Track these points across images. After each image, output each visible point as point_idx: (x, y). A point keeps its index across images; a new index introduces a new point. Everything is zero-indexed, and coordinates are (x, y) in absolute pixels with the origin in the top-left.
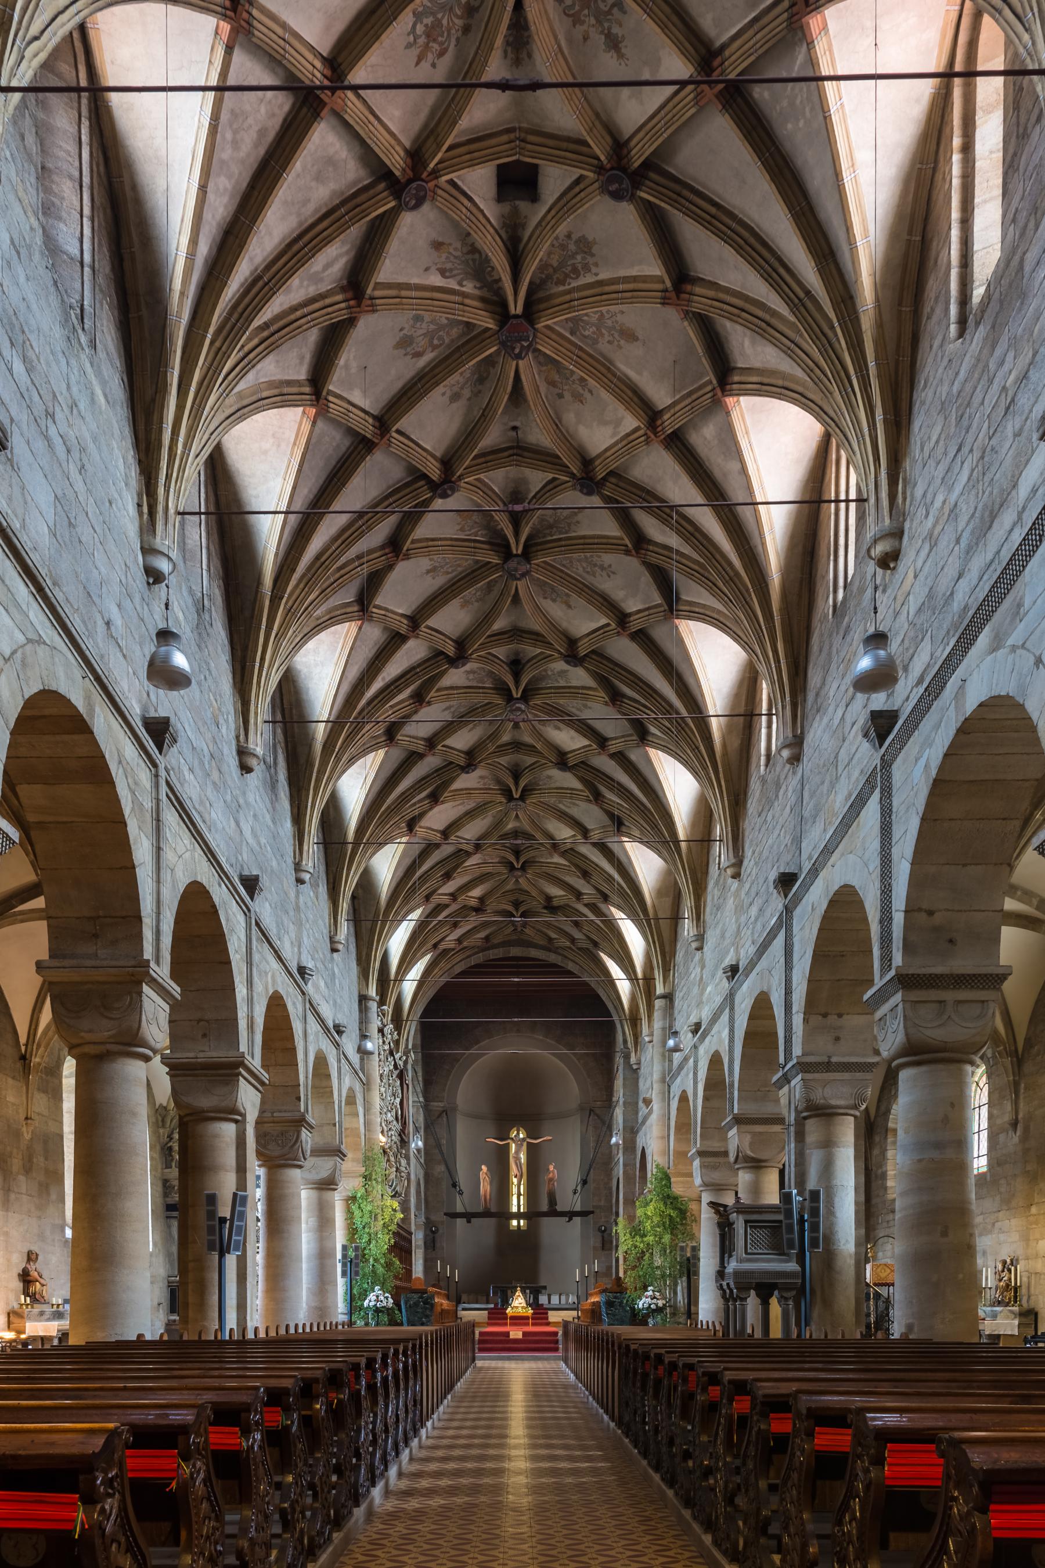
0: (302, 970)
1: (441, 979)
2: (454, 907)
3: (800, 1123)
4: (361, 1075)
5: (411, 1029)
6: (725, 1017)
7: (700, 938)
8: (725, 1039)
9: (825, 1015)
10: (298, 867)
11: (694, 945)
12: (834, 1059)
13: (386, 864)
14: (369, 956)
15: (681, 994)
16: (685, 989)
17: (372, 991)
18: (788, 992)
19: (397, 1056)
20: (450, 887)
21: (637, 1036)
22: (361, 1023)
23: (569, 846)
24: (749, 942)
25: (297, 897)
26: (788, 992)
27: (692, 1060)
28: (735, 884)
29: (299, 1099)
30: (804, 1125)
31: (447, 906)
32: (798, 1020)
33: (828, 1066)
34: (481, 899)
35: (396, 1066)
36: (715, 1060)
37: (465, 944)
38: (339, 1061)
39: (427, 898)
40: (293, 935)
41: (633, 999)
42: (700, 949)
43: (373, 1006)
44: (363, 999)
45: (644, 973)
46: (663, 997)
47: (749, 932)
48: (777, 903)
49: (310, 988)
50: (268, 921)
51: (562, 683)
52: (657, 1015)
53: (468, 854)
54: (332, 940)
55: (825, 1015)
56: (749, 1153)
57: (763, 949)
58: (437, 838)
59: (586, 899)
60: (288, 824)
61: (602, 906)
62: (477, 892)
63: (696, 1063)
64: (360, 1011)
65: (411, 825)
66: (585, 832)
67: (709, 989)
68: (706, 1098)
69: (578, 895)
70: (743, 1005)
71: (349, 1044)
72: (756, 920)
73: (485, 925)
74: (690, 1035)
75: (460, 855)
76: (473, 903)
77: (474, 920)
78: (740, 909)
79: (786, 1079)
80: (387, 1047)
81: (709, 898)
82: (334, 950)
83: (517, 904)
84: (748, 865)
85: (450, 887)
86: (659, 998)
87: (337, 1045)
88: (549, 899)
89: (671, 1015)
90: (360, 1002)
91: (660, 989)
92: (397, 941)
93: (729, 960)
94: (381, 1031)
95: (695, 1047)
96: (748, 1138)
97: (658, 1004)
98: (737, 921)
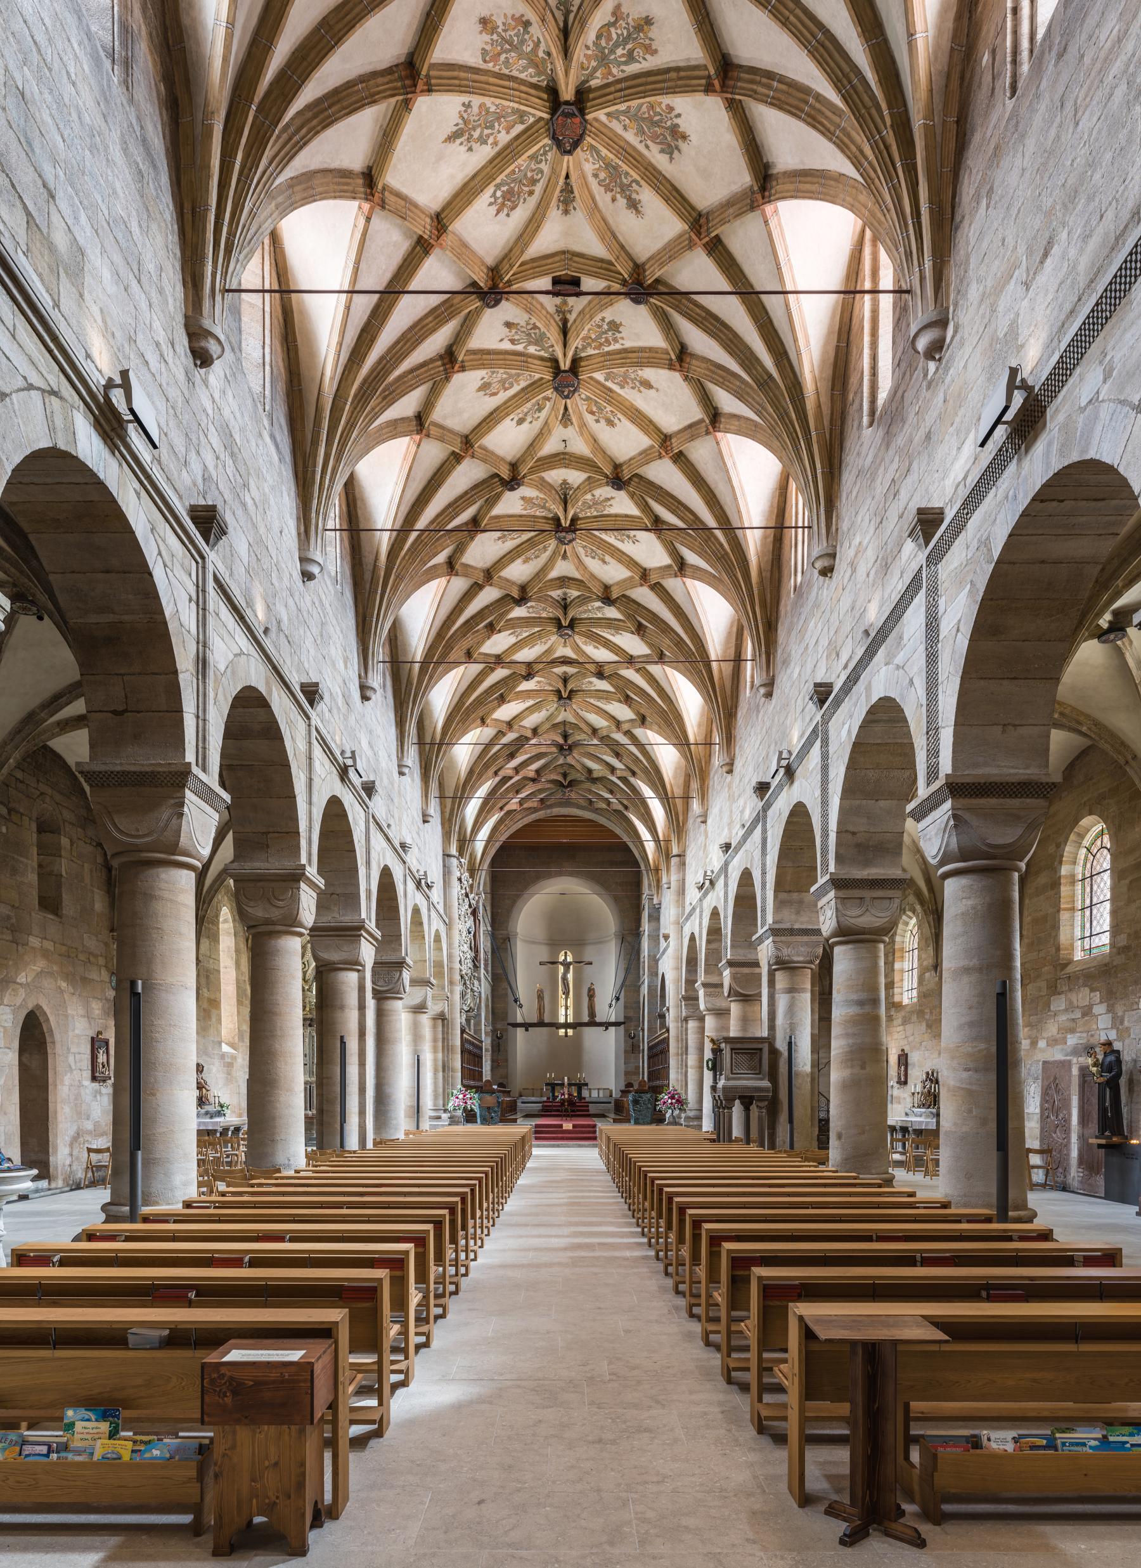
0: (403, 846)
5: (483, 876)
8: (723, 898)
11: (700, 820)
13: (463, 753)
17: (454, 851)
18: (764, 873)
19: (471, 896)
22: (444, 875)
26: (764, 873)
27: (698, 910)
31: (511, 778)
34: (538, 771)
35: (470, 906)
36: (715, 913)
37: (525, 806)
38: (429, 910)
39: (496, 773)
42: (704, 822)
44: (447, 856)
49: (407, 859)
50: (381, 815)
51: (600, 615)
52: (673, 869)
59: (619, 773)
61: (632, 780)
62: (535, 766)
63: (701, 912)
68: (708, 942)
69: (613, 769)
71: (436, 895)
73: (540, 791)
76: (532, 775)
82: (425, 821)
83: (565, 775)
87: (428, 898)
88: (590, 771)
89: (684, 870)
91: (675, 851)
92: (472, 809)
94: (460, 879)
95: (701, 900)
97: (674, 861)
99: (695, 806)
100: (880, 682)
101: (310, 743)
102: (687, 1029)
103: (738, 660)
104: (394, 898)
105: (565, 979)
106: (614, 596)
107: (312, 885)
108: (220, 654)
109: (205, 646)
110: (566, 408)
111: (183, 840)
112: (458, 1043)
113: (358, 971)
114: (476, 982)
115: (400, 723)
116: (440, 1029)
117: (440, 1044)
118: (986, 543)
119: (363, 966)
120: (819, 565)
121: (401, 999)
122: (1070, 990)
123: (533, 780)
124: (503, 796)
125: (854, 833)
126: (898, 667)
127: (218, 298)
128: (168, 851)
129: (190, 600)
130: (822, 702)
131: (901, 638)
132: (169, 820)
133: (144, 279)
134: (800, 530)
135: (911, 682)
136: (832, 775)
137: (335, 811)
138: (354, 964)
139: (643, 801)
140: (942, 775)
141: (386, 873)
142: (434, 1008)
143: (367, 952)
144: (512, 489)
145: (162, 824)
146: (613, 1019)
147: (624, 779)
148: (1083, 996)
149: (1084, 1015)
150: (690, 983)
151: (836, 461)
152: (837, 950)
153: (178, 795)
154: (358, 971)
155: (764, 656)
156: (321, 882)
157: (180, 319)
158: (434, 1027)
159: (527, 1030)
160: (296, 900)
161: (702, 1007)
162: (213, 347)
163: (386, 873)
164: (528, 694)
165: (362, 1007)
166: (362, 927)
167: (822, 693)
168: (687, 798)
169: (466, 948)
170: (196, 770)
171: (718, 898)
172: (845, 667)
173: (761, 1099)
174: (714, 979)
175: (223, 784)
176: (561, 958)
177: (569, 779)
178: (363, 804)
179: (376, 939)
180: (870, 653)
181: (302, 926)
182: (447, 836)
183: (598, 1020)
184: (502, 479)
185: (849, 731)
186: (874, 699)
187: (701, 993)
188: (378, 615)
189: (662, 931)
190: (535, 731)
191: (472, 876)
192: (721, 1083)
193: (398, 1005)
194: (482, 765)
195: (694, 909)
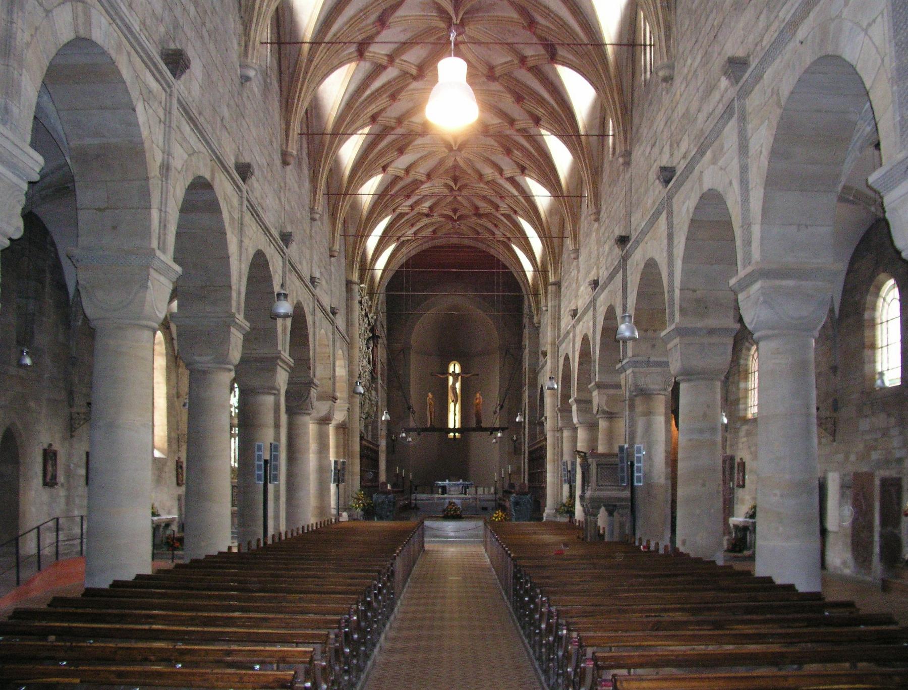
0: (313, 280)
1: (402, 258)
4: (347, 337)
5: (381, 297)
6: (591, 312)
7: (577, 251)
10: (312, 210)
11: (572, 256)
12: (652, 359)
14: (353, 252)
17: (355, 277)
19: (370, 316)
20: (410, 202)
21: (538, 303)
22: (347, 300)
23: (490, 178)
24: (604, 268)
25: (311, 230)
27: (571, 335)
28: (596, 225)
29: (309, 368)
31: (407, 214)
33: (648, 363)
34: (431, 208)
35: (369, 324)
36: (585, 339)
39: (394, 210)
40: (308, 257)
41: (534, 278)
42: (577, 258)
43: (356, 288)
44: (349, 284)
48: (617, 251)
49: (317, 292)
50: (295, 258)
53: (422, 183)
54: (331, 250)
57: (611, 277)
58: (402, 173)
60: (307, 185)
61: (514, 216)
63: (574, 337)
64: (347, 292)
65: (384, 168)
66: (501, 171)
67: (582, 288)
68: (580, 364)
70: (601, 309)
71: (340, 321)
72: (609, 254)
73: (433, 224)
75: (417, 183)
76: (426, 211)
77: (425, 221)
78: (598, 241)
80: (363, 313)
82: (331, 256)
83: (455, 211)
84: (603, 215)
85: (410, 202)
88: (477, 208)
89: (560, 297)
90: (347, 285)
91: (552, 279)
92: (372, 243)
93: (592, 276)
94: (360, 302)
95: (574, 326)
96: (605, 398)
99: (569, 243)
102: (562, 438)
103: (603, 135)
105: (454, 388)
106: (497, 74)
107: (240, 328)
108: (179, 157)
111: (147, 308)
112: (357, 448)
113: (275, 394)
114: (374, 393)
115: (314, 179)
118: (776, 92)
119: (279, 390)
121: (309, 414)
122: (873, 414)
124: (399, 229)
125: (694, 291)
129: (160, 121)
130: (667, 182)
131: (722, 148)
134: (648, 48)
135: (731, 183)
136: (676, 242)
137: (259, 263)
138: (272, 390)
140: (753, 261)
143: (282, 378)
148: (880, 420)
149: (884, 435)
150: (566, 396)
152: (683, 386)
154: (275, 394)
155: (622, 134)
156: (247, 325)
159: (419, 434)
161: (575, 420)
165: (277, 426)
166: (279, 358)
167: (667, 175)
168: (562, 238)
169: (365, 362)
170: (158, 253)
171: (588, 328)
172: (684, 157)
173: (622, 507)
175: (175, 260)
176: (451, 369)
177: (458, 214)
178: (282, 254)
180: (701, 152)
182: (350, 266)
183: (484, 425)
185: (688, 210)
186: (705, 189)
187: (574, 408)
188: (299, 97)
191: (371, 299)
192: (588, 494)
194: (382, 199)
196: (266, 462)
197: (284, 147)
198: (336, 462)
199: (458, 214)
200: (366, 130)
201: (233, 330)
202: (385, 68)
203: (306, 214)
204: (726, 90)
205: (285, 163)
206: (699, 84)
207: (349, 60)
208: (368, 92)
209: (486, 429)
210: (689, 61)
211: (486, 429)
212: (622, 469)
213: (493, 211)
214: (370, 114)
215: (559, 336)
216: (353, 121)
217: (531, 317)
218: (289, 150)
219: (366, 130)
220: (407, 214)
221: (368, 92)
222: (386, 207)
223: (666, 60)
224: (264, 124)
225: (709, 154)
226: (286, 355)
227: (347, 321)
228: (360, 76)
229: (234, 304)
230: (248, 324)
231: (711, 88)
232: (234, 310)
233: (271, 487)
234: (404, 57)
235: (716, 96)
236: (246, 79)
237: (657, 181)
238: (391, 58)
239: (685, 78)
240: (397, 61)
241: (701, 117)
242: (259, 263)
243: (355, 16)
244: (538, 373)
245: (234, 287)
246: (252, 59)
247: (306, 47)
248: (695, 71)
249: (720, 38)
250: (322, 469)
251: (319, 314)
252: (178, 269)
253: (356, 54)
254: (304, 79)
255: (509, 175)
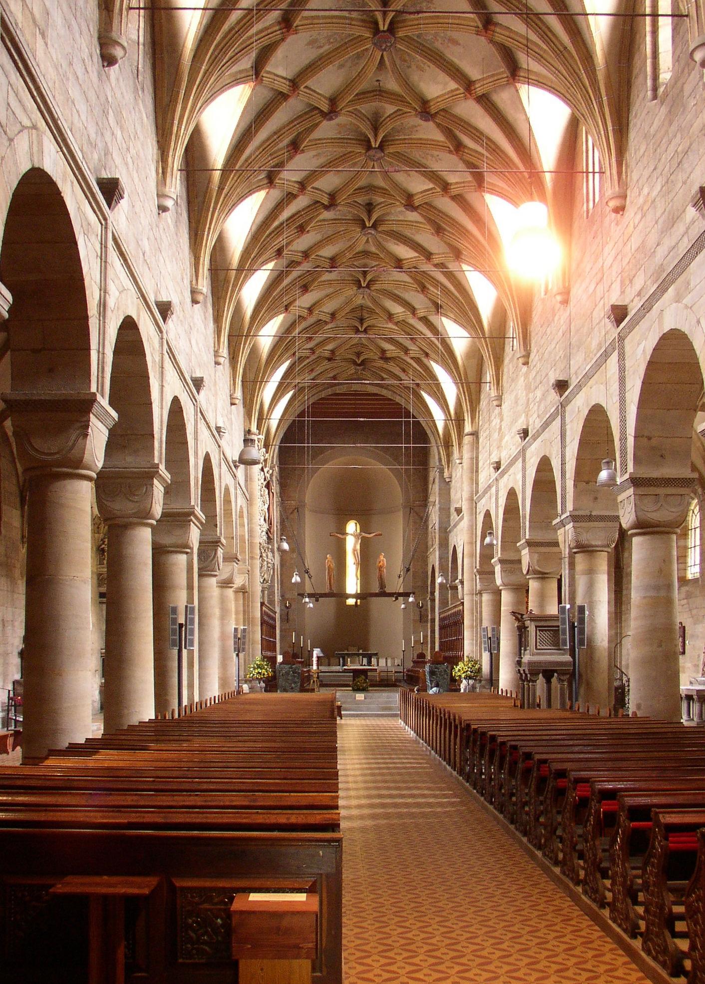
0: (218, 429)
2: (313, 357)
3: (572, 556)
7: (500, 398)
9: (587, 483)
11: (495, 403)
13: (267, 335)
14: (252, 401)
15: (485, 435)
16: (487, 432)
17: (254, 428)
18: (563, 464)
19: (266, 470)
21: (449, 455)
23: (401, 318)
24: (535, 416)
26: (563, 464)
27: (494, 489)
28: (525, 368)
29: (216, 526)
30: (574, 558)
31: (308, 357)
32: (570, 484)
34: (333, 352)
35: (265, 480)
36: (512, 494)
38: (236, 489)
41: (446, 427)
42: (499, 406)
45: (456, 413)
46: (472, 434)
47: (536, 408)
48: (553, 396)
49: (223, 443)
53: (326, 323)
55: (587, 483)
56: (537, 568)
57: (546, 425)
60: (211, 325)
61: (425, 360)
65: (287, 308)
66: (413, 310)
67: (506, 438)
68: (505, 520)
69: (406, 351)
70: (532, 460)
74: (492, 470)
78: (529, 388)
79: (563, 524)
81: (505, 370)
82: (232, 404)
86: (468, 435)
88: (383, 351)
89: (477, 448)
91: (468, 428)
93: (520, 424)
96: (536, 556)
97: (467, 440)
98: (527, 395)
100: (669, 316)
101: (162, 354)
102: (481, 602)
104: (212, 481)
107: (162, 480)
109: (105, 292)
110: (382, 56)
112: (258, 614)
113: (187, 553)
114: (270, 554)
115: (218, 319)
116: (241, 602)
117: (241, 616)
119: (192, 549)
120: (613, 204)
121: (215, 576)
123: (329, 359)
126: (686, 307)
127: (124, 12)
128: (72, 465)
131: (689, 284)
132: (76, 440)
133: (78, 14)
136: (628, 386)
137: (176, 408)
138: (183, 547)
139: (434, 377)
141: (207, 459)
142: (239, 581)
143: (194, 535)
144: (331, 119)
145: (70, 444)
146: (401, 591)
147: (418, 360)
151: (624, 121)
152: (636, 540)
153: (85, 419)
154: (187, 553)
156: (167, 476)
157: (96, 35)
158: (236, 600)
159: (317, 600)
160: (149, 494)
161: (499, 582)
162: (118, 52)
163: (207, 459)
164: (330, 282)
165: (190, 587)
166: (193, 513)
173: (561, 673)
174: (511, 556)
178: (194, 399)
179: (201, 523)
180: (662, 289)
181: (152, 518)
182: (248, 414)
183: (388, 590)
184: (321, 111)
187: (498, 569)
188: (209, 228)
189: (454, 506)
190: (333, 315)
192: (526, 658)
193: (213, 581)
194: (282, 344)
195: (490, 487)
196: (181, 625)
197: (194, 282)
198: (236, 630)
199: (361, 359)
200: (271, 265)
201: (155, 481)
202: (295, 196)
203: (212, 359)
204: (693, 222)
205: (195, 302)
206: (658, 214)
207: (258, 188)
208: (276, 223)
209: (390, 595)
210: (646, 191)
211: (390, 595)
212: (564, 630)
213: (402, 354)
214: (277, 247)
215: (477, 492)
216: (259, 255)
217: (442, 472)
218: (200, 287)
219: (271, 265)
220: (308, 357)
221: (276, 223)
222: (287, 349)
223: (617, 188)
224: (176, 259)
225: (671, 291)
226: (198, 511)
227: (246, 476)
228: (270, 205)
229: (156, 453)
230: (169, 476)
231: (673, 220)
232: (156, 461)
233: (185, 652)
234: (315, 185)
235: (680, 228)
236: (162, 209)
237: (607, 320)
238: (303, 185)
239: (641, 208)
240: (309, 189)
241: (661, 251)
242: (176, 408)
243: (268, 139)
244: (450, 532)
245: (156, 436)
246: (171, 187)
247: (217, 175)
248: (653, 201)
249: (686, 165)
250: (223, 637)
251: (224, 467)
252: (115, 415)
253: (266, 181)
254: (215, 209)
255: (422, 315)
